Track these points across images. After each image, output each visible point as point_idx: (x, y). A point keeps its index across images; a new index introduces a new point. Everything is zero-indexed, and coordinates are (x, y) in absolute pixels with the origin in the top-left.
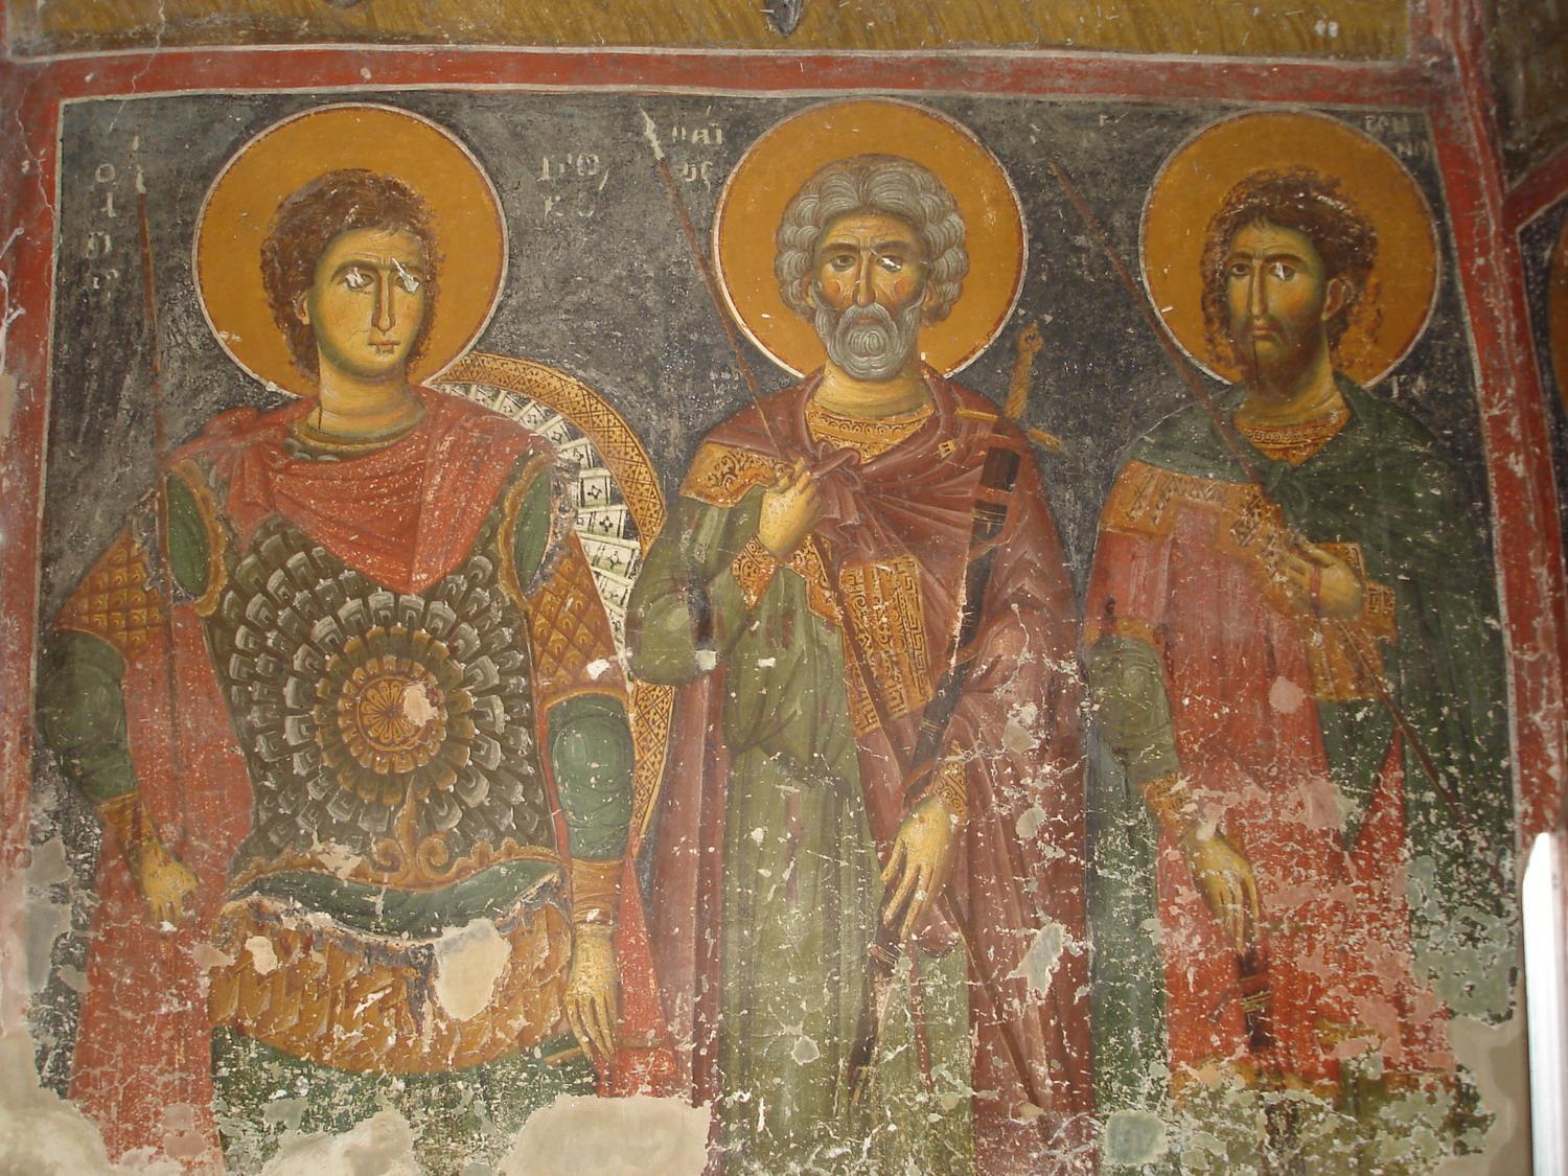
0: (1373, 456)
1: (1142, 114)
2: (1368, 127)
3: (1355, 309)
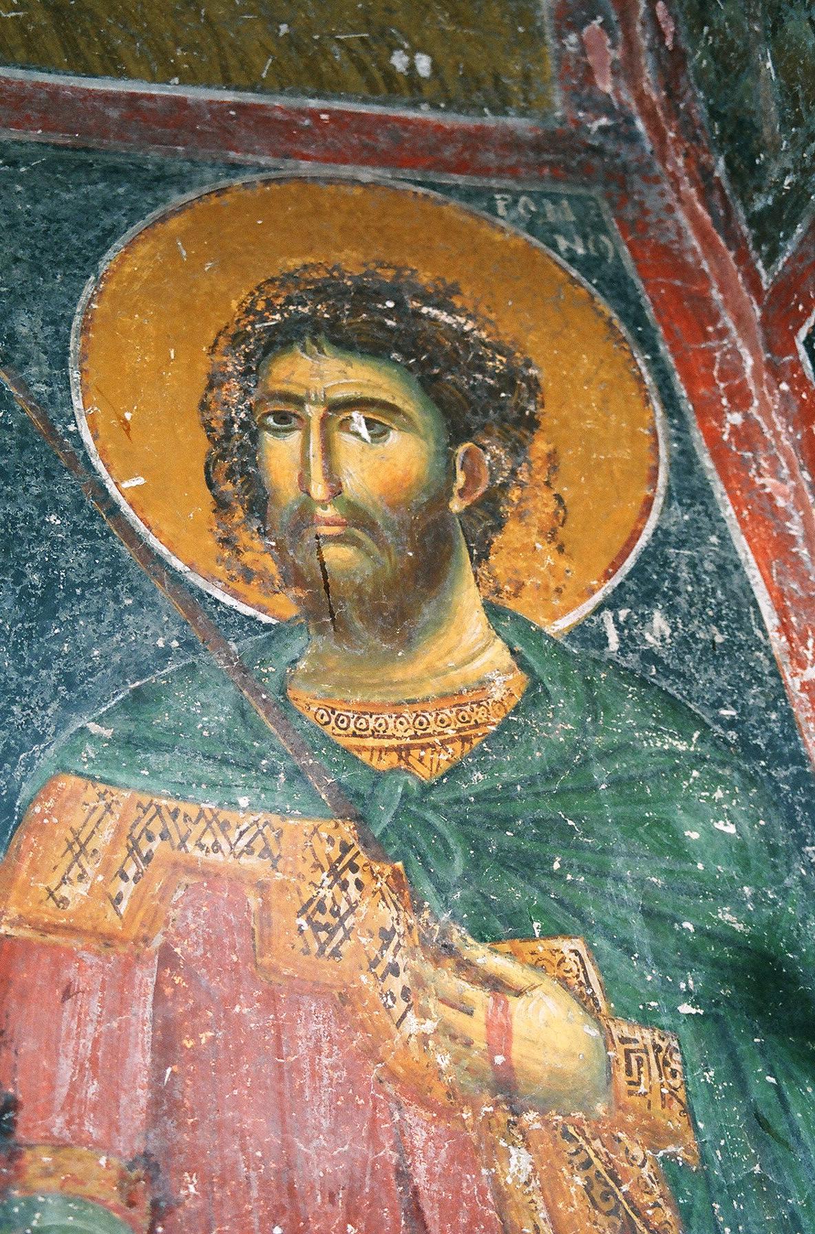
0: (586, 762)
1: (70, 164)
2: (501, 211)
3: (514, 494)
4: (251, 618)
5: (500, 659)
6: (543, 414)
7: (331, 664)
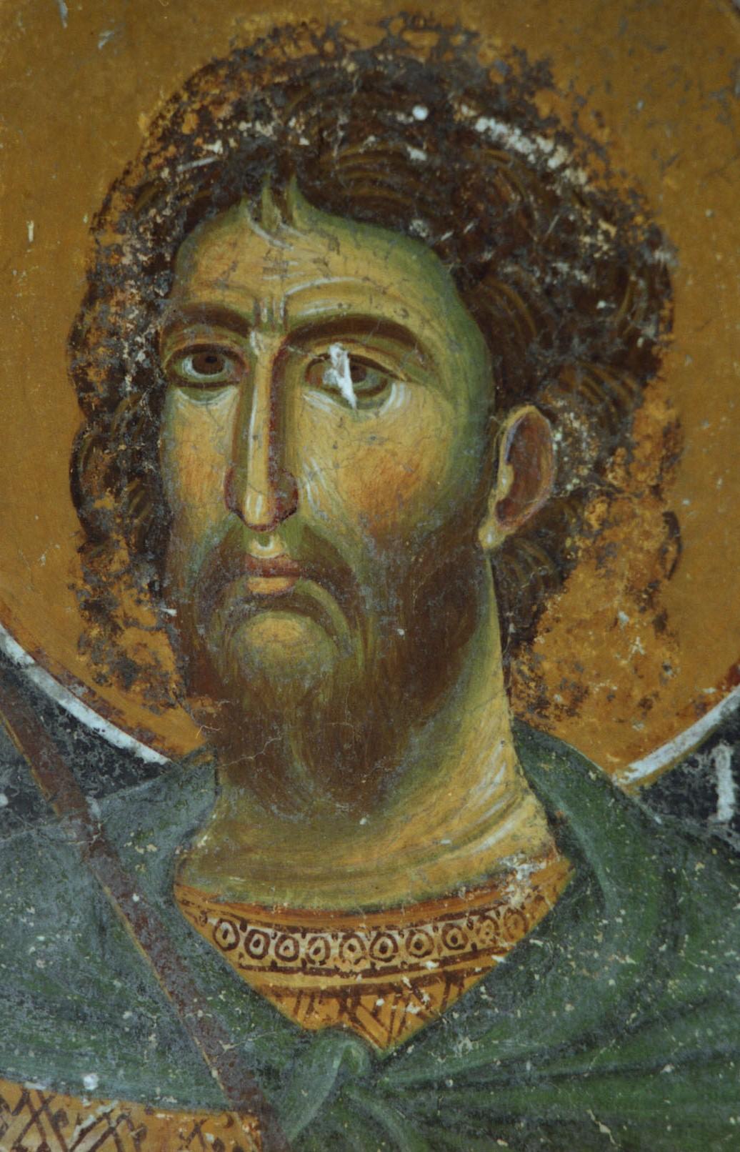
3: (595, 512)
4: (126, 754)
5: (528, 831)
6: (668, 343)
7: (248, 839)
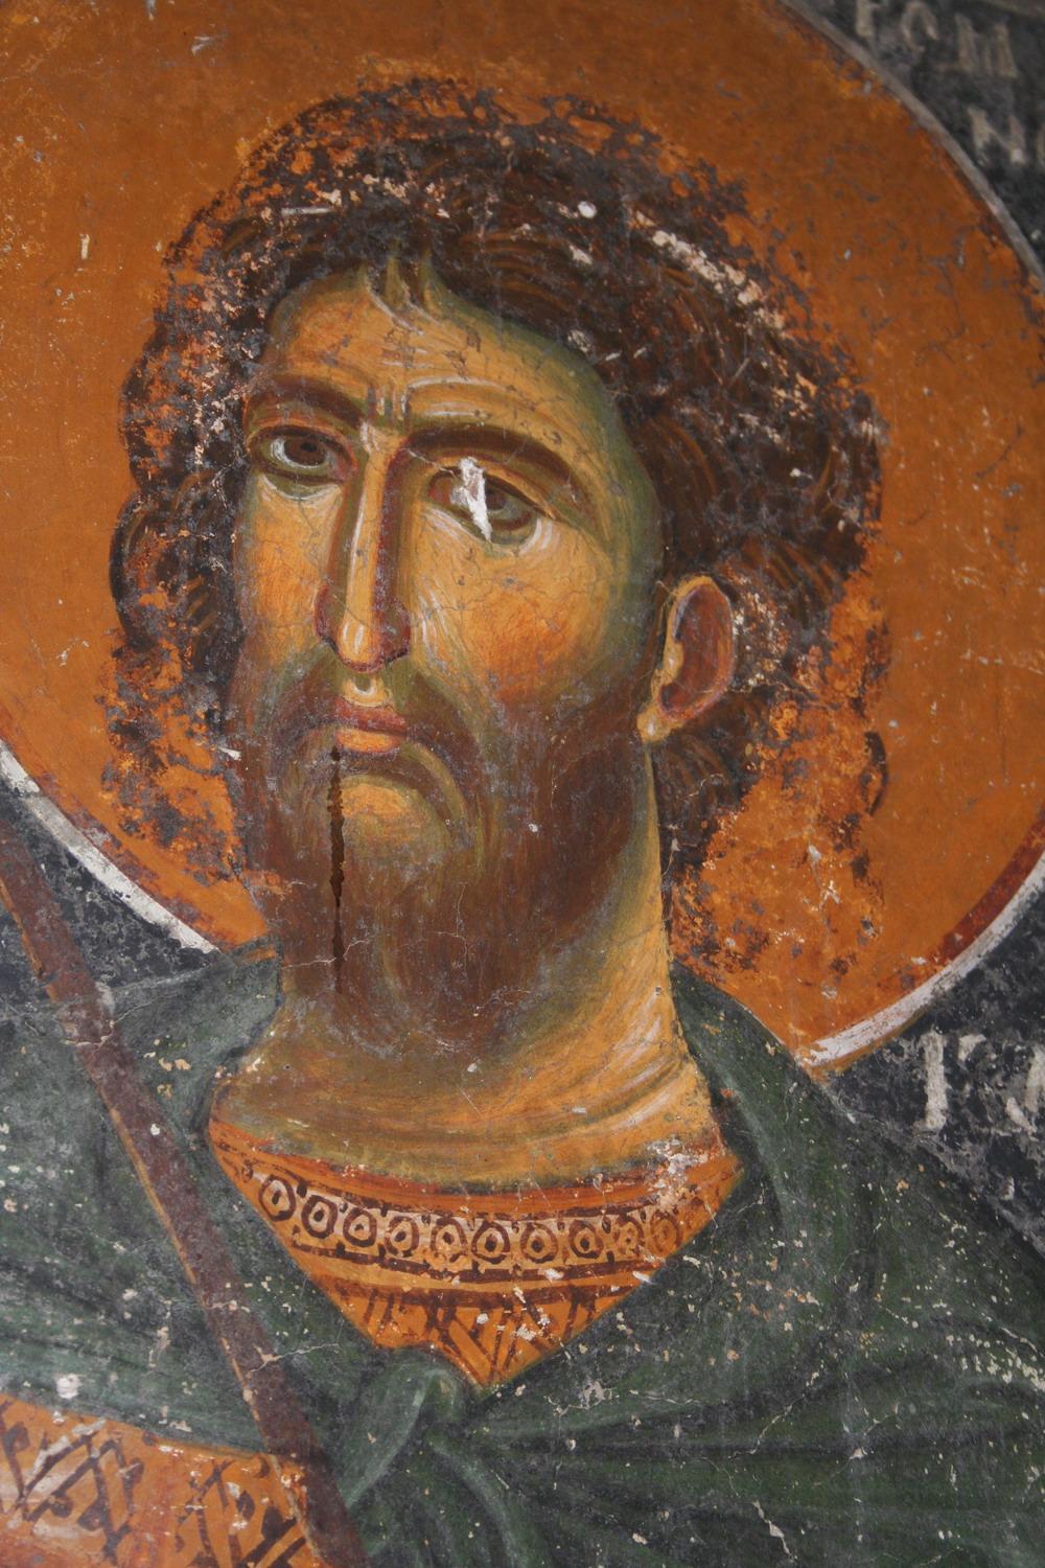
0: (831, 1388)
2: (863, 26)
3: (783, 718)
4: (158, 932)
5: (686, 1111)
6: (875, 533)
7: (317, 1072)
